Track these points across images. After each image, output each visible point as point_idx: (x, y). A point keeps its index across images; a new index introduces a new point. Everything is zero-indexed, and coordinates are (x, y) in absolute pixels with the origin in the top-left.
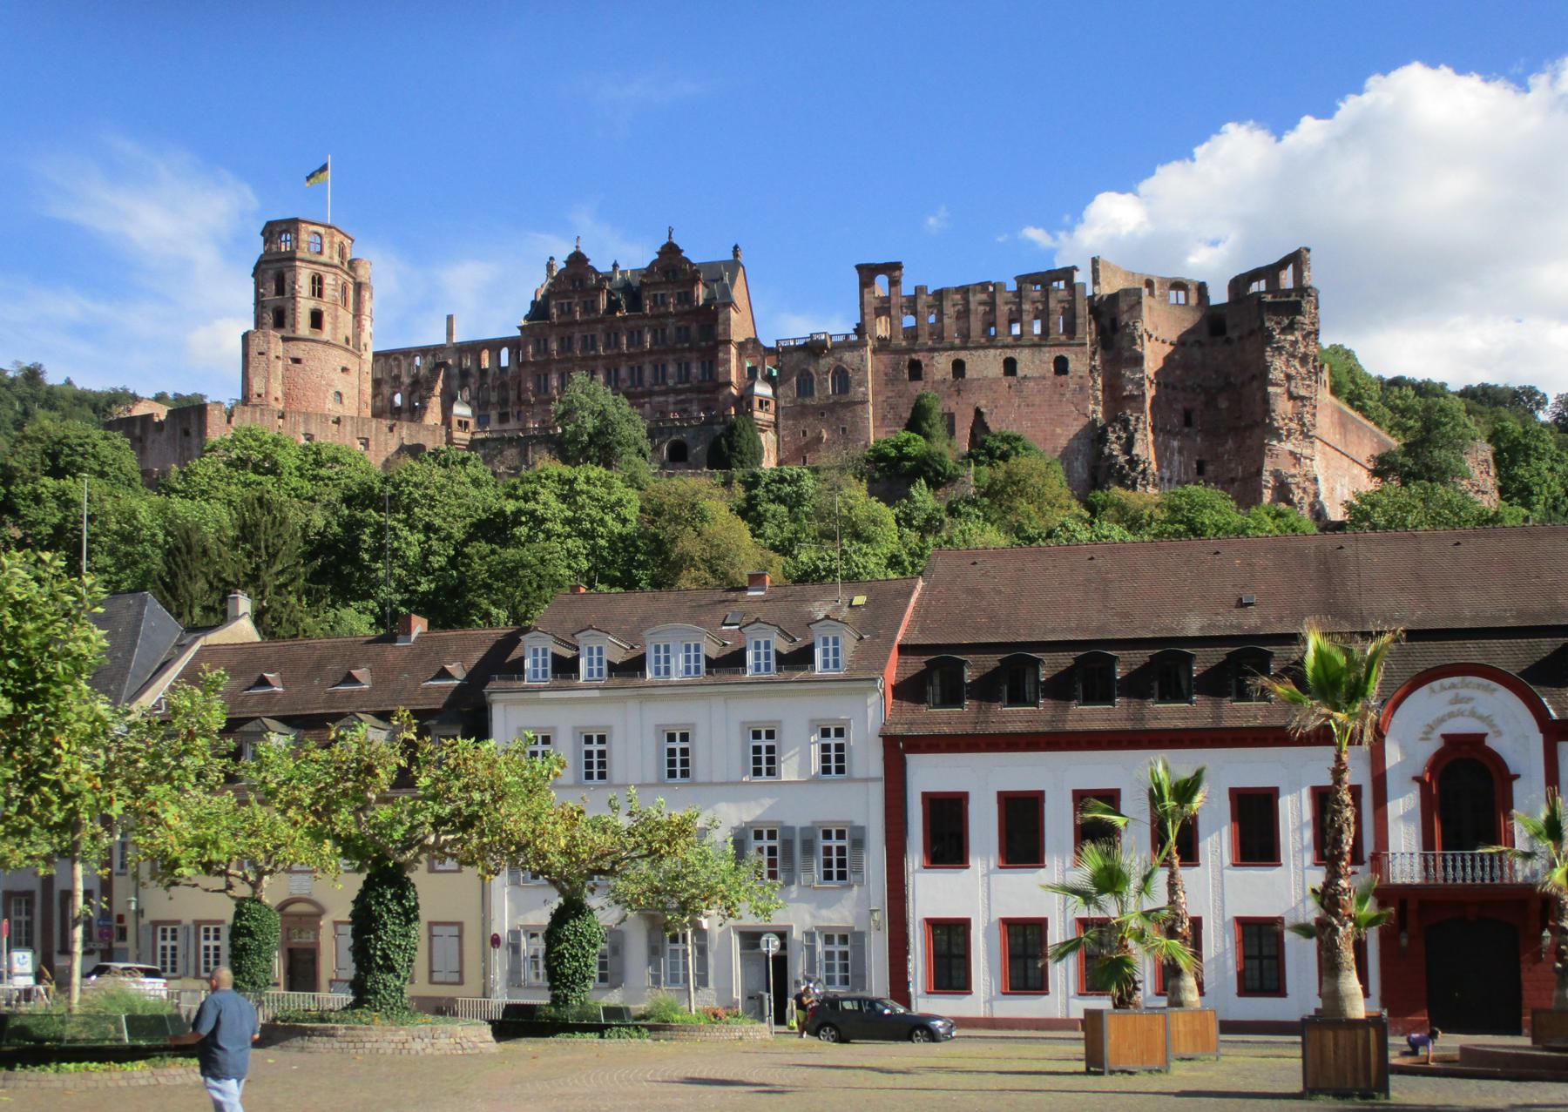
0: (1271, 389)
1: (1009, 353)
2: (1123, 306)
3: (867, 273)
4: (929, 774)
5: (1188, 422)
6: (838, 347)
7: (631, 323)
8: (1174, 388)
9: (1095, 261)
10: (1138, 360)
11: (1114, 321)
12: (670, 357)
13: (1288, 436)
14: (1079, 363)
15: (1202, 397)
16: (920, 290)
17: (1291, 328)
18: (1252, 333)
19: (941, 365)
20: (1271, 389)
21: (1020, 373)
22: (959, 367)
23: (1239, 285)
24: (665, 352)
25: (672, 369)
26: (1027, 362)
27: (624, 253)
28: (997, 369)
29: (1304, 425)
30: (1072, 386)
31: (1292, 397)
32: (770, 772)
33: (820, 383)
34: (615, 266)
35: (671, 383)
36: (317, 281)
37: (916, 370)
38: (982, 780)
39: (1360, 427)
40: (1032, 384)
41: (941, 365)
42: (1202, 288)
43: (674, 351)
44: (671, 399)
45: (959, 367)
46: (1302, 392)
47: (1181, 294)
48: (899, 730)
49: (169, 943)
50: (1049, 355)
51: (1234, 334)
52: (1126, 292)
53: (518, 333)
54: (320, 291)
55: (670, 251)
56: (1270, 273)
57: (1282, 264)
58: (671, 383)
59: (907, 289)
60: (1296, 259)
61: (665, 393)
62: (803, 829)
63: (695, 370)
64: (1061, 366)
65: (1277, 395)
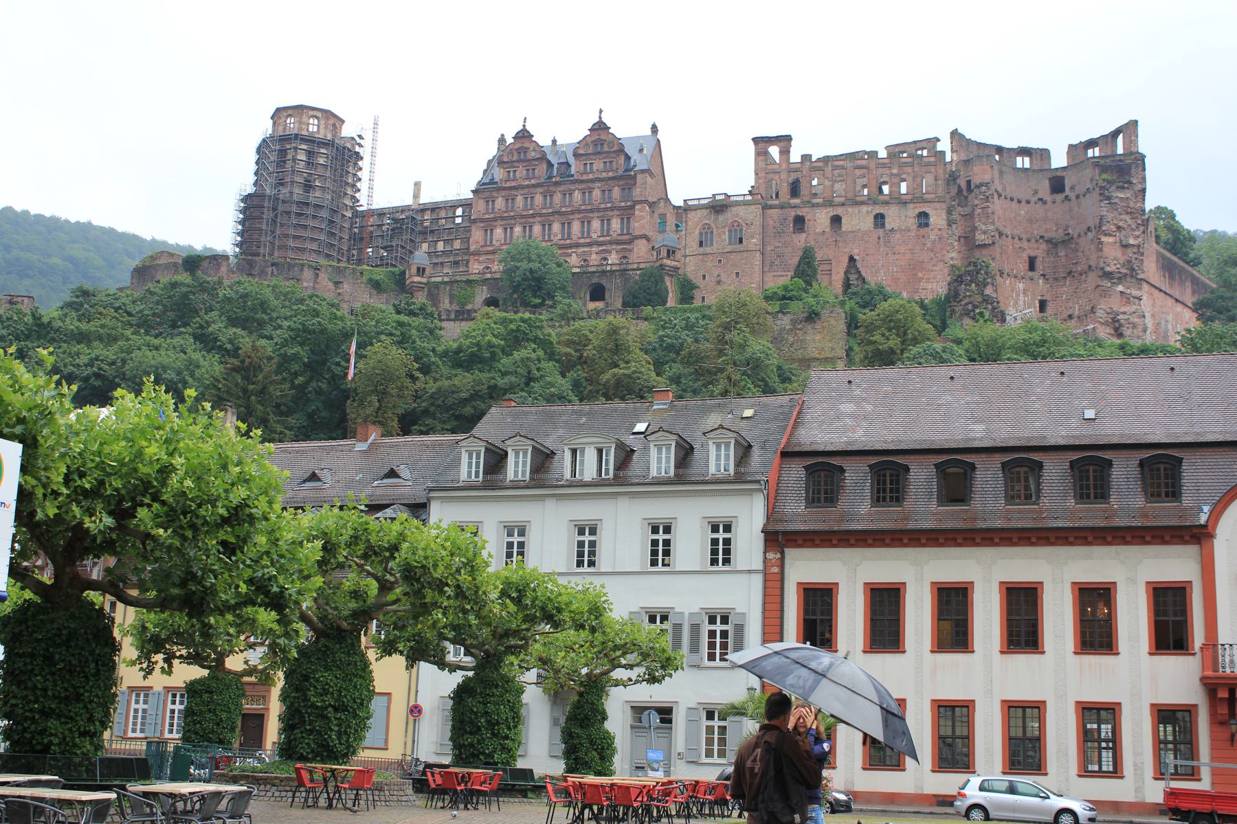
1: (879, 209)
3: (762, 143)
4: (806, 567)
5: (1032, 267)
6: (737, 203)
7: (563, 188)
8: (1020, 239)
9: (955, 134)
10: (988, 216)
11: (969, 182)
12: (596, 214)
14: (938, 218)
15: (1044, 246)
19: (820, 219)
21: (888, 227)
22: (836, 220)
24: (592, 211)
25: (596, 224)
26: (894, 217)
27: (561, 130)
28: (869, 223)
29: (1132, 269)
30: (932, 237)
32: (664, 565)
33: (720, 235)
34: (554, 141)
35: (594, 236)
37: (800, 222)
38: (851, 575)
39: (1182, 271)
40: (898, 236)
41: (820, 219)
43: (598, 210)
44: (595, 249)
45: (836, 220)
46: (1132, 241)
47: (1027, 160)
49: (141, 706)
50: (913, 211)
51: (1072, 196)
53: (471, 196)
55: (600, 127)
57: (1115, 134)
58: (594, 236)
59: (795, 157)
61: (590, 245)
62: (691, 614)
63: (616, 224)
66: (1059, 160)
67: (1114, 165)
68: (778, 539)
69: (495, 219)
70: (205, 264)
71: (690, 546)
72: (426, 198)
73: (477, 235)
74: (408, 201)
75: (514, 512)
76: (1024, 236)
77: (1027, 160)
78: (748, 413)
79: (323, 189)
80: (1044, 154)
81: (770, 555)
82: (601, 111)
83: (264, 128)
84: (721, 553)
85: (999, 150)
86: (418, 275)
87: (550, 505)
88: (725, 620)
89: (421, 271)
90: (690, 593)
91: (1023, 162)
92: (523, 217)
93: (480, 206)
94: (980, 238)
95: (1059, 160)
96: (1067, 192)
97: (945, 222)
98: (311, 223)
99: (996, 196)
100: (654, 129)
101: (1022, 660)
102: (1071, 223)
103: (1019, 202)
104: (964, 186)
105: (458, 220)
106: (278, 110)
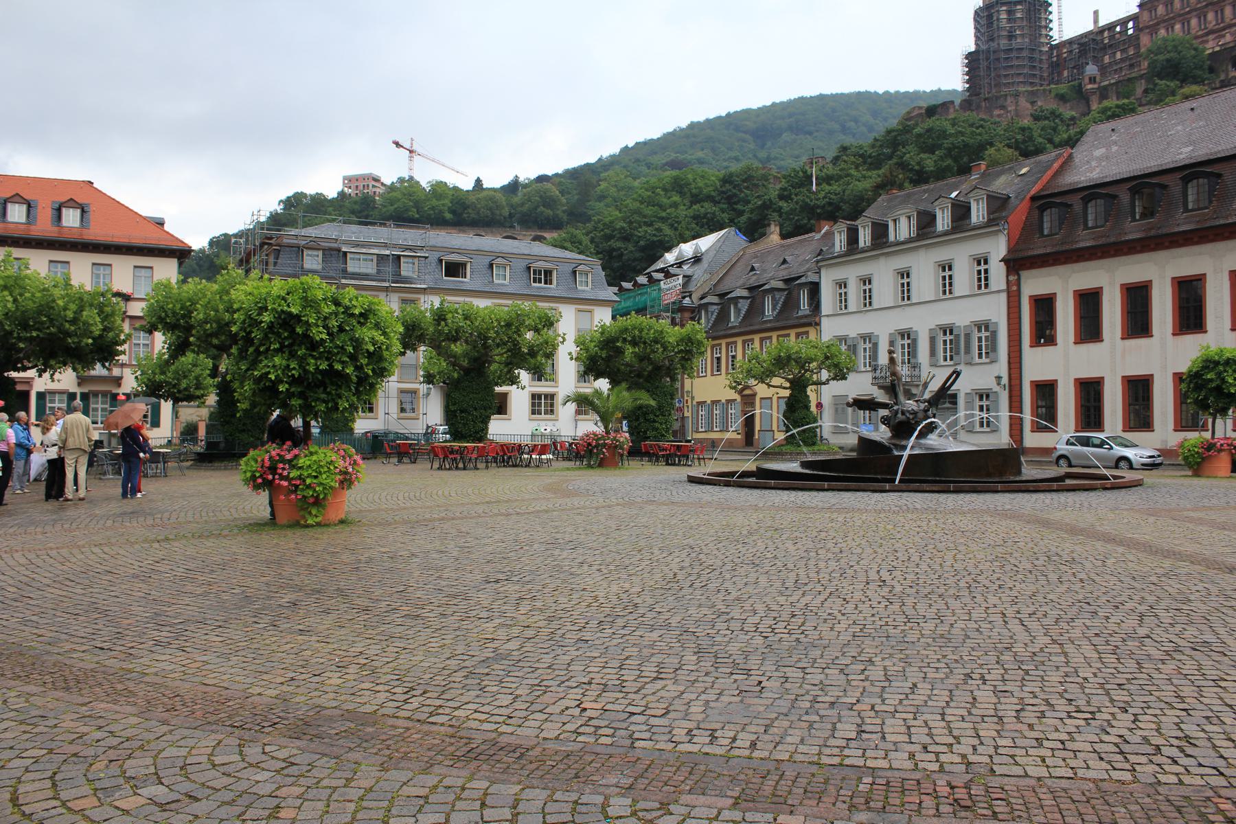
4: (1035, 284)
38: (1062, 284)
48: (1011, 257)
53: (1137, 10)
68: (1016, 264)
69: (1158, 24)
70: (939, 110)
71: (963, 278)
72: (1102, 22)
73: (1145, 40)
74: (1090, 27)
75: (863, 269)
78: (1024, 171)
79: (1022, 36)
81: (1011, 278)
84: (983, 279)
86: (1090, 83)
87: (882, 260)
88: (987, 329)
89: (1092, 80)
90: (962, 314)
92: (1180, 15)
93: (1146, 16)
98: (1016, 63)
105: (1130, 32)
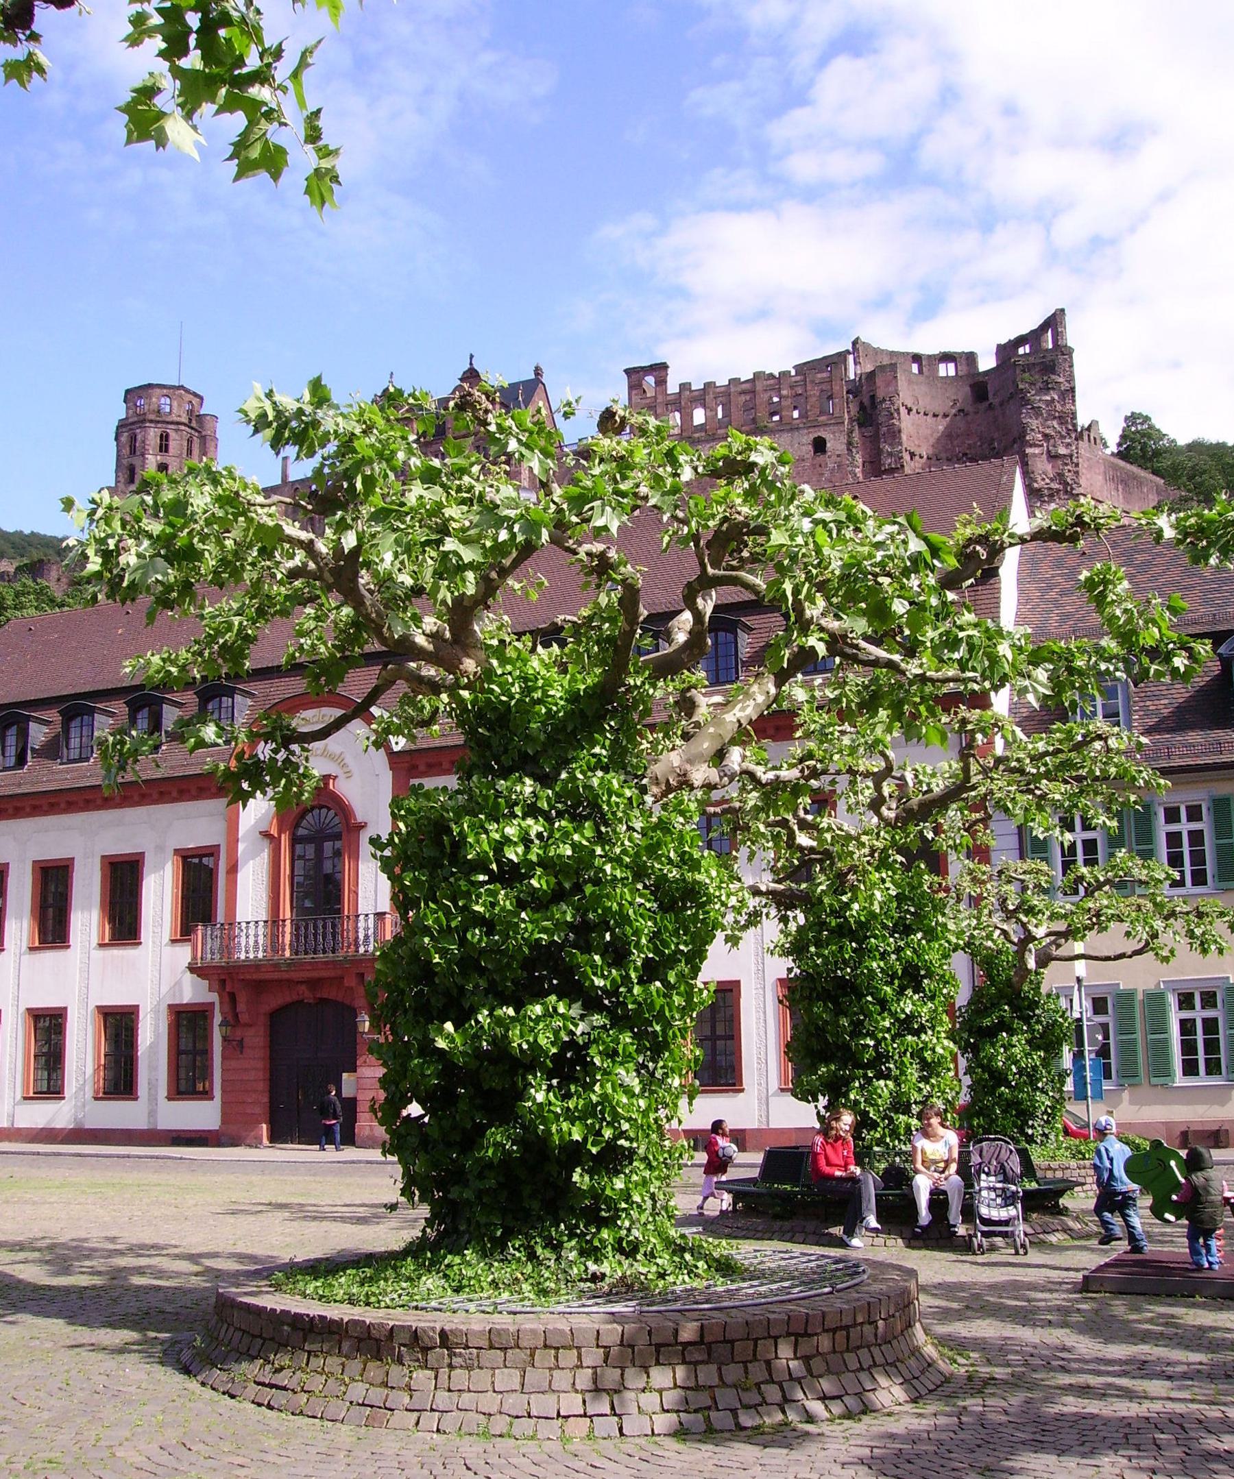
0: (1029, 451)
2: (879, 381)
10: (895, 434)
11: (873, 397)
13: (1051, 496)
16: (684, 387)
17: (1046, 389)
18: (1012, 396)
20: (1029, 451)
23: (1006, 351)
31: (1053, 457)
36: (164, 438)
39: (1140, 483)
42: (971, 358)
46: (1062, 451)
47: (951, 366)
52: (882, 368)
54: (167, 446)
56: (1033, 337)
59: (672, 388)
60: (1054, 322)
64: (819, 445)
65: (1035, 455)
66: (987, 362)
67: (1038, 361)
76: (943, 455)
77: (951, 366)
80: (971, 358)
82: (472, 357)
83: (121, 412)
85: (917, 358)
91: (947, 370)
94: (888, 462)
95: (987, 362)
96: (991, 401)
97: (844, 447)
99: (903, 411)
100: (538, 371)
101: (50, 957)
102: (996, 435)
103: (935, 415)
104: (866, 401)
106: (128, 392)
